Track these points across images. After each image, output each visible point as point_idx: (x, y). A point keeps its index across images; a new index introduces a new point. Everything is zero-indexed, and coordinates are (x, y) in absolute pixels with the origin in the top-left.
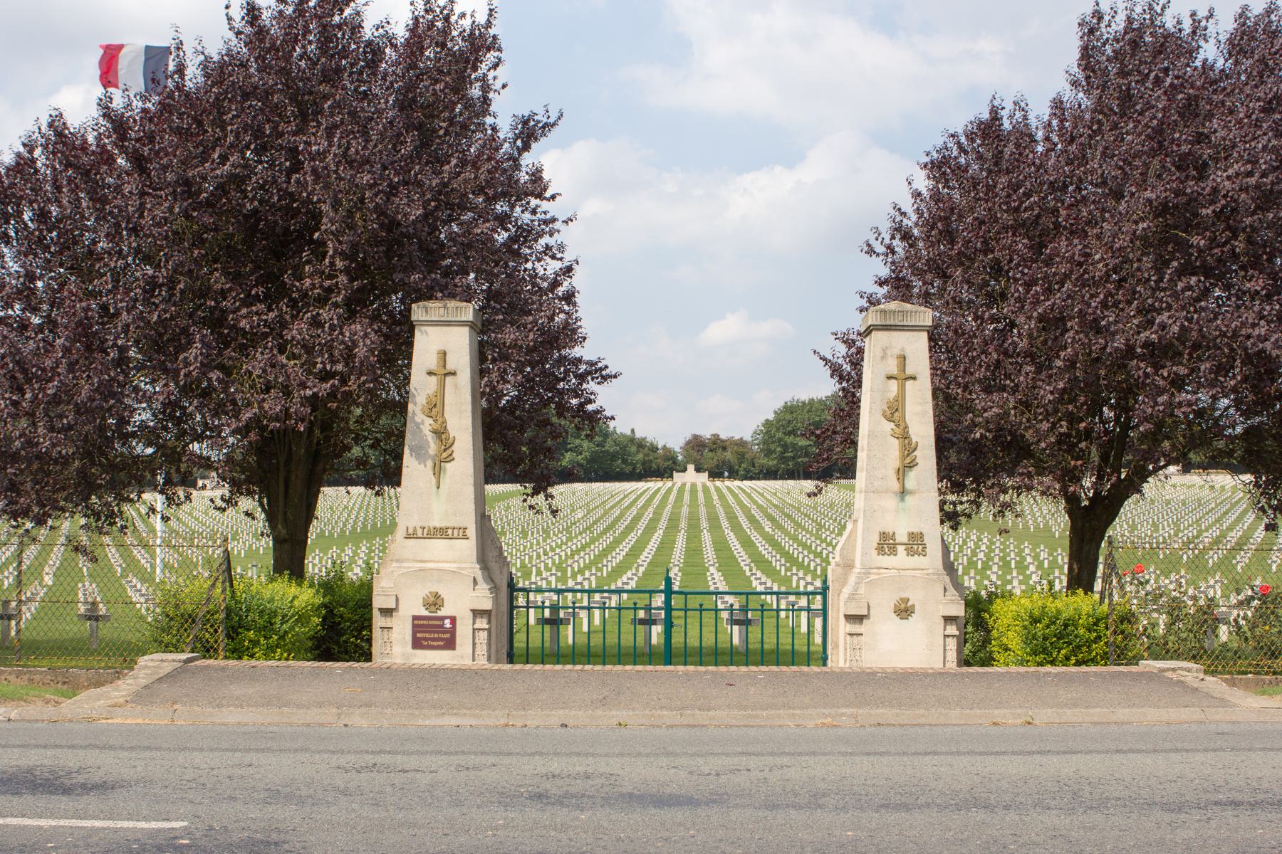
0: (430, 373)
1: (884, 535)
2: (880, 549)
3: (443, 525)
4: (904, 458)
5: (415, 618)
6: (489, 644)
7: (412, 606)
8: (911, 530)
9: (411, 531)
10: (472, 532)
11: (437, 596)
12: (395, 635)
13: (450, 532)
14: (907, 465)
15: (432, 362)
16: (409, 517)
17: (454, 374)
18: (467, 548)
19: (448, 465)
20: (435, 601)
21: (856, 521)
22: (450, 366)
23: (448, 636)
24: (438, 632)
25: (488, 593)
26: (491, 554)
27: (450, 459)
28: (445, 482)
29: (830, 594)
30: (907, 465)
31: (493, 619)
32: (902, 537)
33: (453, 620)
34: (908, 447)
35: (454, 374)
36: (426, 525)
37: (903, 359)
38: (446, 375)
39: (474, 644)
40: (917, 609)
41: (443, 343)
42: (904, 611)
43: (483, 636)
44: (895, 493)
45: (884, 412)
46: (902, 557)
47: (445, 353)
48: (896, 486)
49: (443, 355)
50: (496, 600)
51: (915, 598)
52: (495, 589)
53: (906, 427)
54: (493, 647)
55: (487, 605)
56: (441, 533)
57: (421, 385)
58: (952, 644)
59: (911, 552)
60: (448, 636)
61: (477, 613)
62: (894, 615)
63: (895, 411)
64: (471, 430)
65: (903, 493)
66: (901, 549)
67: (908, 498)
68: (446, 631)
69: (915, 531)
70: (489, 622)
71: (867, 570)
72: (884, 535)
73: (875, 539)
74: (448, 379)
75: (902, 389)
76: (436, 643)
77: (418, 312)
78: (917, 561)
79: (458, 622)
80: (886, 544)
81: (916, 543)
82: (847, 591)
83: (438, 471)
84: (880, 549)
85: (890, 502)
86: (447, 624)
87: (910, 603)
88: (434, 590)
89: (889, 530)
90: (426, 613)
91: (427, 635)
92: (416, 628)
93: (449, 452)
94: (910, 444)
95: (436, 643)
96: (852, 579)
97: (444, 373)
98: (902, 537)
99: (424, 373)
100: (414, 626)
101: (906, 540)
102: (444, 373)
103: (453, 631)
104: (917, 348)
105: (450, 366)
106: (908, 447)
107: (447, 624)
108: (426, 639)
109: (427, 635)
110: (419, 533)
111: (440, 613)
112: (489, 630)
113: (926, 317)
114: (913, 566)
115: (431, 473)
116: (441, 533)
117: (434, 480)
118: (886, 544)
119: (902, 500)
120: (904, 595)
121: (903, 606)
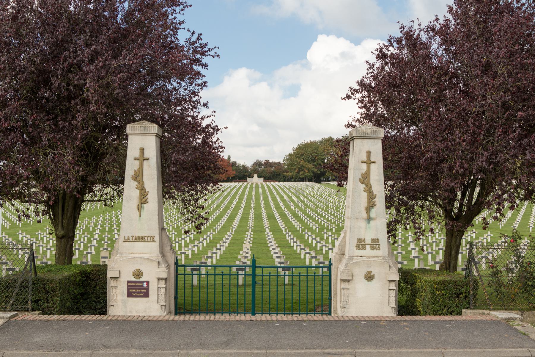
0: (136, 159)
1: (359, 240)
2: (358, 247)
3: (143, 235)
4: (369, 202)
5: (129, 282)
6: (166, 294)
7: (128, 276)
8: (373, 237)
9: (126, 238)
10: (157, 238)
11: (139, 270)
12: (119, 290)
13: (146, 238)
14: (371, 205)
15: (137, 154)
16: (127, 230)
17: (147, 159)
18: (155, 247)
19: (145, 205)
20: (138, 274)
21: (346, 232)
23: (145, 291)
24: (140, 289)
25: (165, 269)
26: (167, 248)
27: (146, 202)
29: (333, 267)
30: (371, 205)
31: (168, 281)
32: (368, 241)
33: (148, 283)
34: (371, 196)
35: (147, 159)
36: (134, 235)
37: (369, 153)
39: (158, 295)
40: (376, 276)
41: (142, 143)
42: (369, 277)
43: (163, 290)
44: (365, 219)
45: (360, 180)
46: (368, 251)
48: (365, 215)
49: (142, 150)
50: (169, 272)
51: (375, 271)
52: (168, 267)
53: (371, 187)
54: (168, 295)
55: (165, 275)
56: (141, 239)
58: (393, 294)
59: (373, 248)
60: (145, 291)
61: (159, 279)
62: (364, 280)
63: (365, 179)
64: (156, 188)
65: (369, 219)
66: (368, 247)
67: (371, 222)
68: (144, 288)
69: (375, 238)
70: (166, 283)
71: (351, 258)
72: (359, 240)
73: (356, 241)
74: (145, 162)
75: (369, 168)
76: (139, 295)
78: (375, 253)
79: (150, 284)
80: (361, 244)
81: (375, 244)
82: (342, 267)
83: (140, 208)
84: (358, 247)
85: (363, 224)
86: (145, 285)
87: (372, 274)
89: (363, 238)
90: (134, 279)
91: (135, 291)
92: (129, 287)
93: (145, 198)
94: (372, 195)
95: (139, 295)
96: (344, 261)
97: (142, 158)
98: (368, 241)
99: (133, 159)
100: (128, 286)
101: (370, 243)
102: (142, 158)
103: (147, 288)
104: (376, 148)
105: (146, 155)
106: (371, 196)
107: (145, 285)
108: (134, 293)
109: (135, 291)
110: (131, 239)
111: (141, 280)
112: (166, 288)
113: (381, 132)
114: (374, 255)
115: (137, 210)
116: (141, 239)
117: (138, 213)
118: (361, 244)
119: (369, 223)
120: (369, 270)
121: (369, 275)
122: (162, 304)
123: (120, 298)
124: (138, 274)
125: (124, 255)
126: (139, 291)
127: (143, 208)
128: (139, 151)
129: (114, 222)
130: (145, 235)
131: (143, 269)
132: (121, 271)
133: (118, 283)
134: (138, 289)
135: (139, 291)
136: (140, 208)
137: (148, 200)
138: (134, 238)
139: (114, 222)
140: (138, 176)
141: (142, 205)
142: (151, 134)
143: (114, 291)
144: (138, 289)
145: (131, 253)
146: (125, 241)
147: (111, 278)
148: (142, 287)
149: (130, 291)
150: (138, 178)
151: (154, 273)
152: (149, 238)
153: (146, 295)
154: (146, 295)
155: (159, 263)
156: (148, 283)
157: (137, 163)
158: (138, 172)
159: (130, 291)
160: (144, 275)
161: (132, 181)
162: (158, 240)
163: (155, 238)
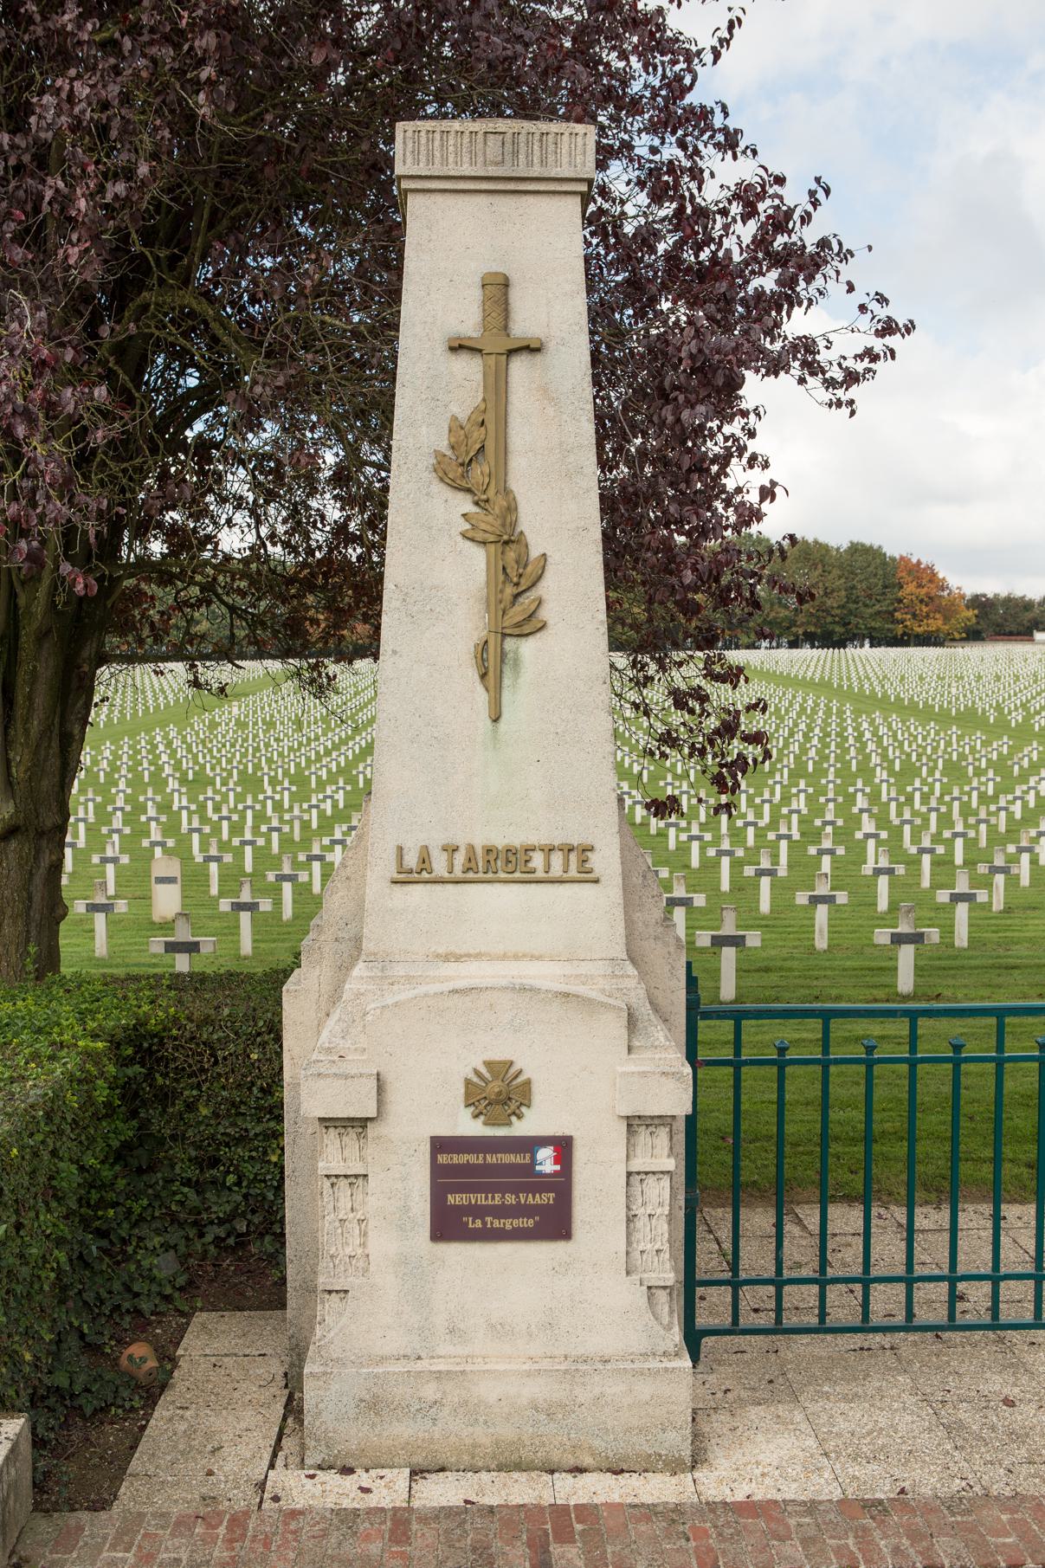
0: (458, 347)
3: (517, 839)
5: (440, 1145)
9: (411, 860)
10: (607, 860)
11: (500, 1069)
12: (375, 1199)
13: (538, 860)
15: (467, 319)
16: (407, 811)
19: (527, 649)
20: (500, 1092)
22: (524, 324)
23: (548, 1198)
24: (516, 1189)
27: (530, 625)
28: (519, 698)
33: (563, 1147)
36: (462, 842)
38: (511, 352)
39: (631, 1219)
47: (506, 284)
49: (498, 290)
56: (504, 864)
57: (430, 391)
60: (548, 1198)
61: (634, 1123)
68: (542, 1184)
74: (519, 366)
76: (508, 1224)
77: (417, 147)
79: (580, 1156)
83: (492, 666)
86: (546, 1161)
88: (498, 1055)
90: (469, 1126)
91: (480, 1199)
93: (526, 600)
95: (508, 1224)
97: (500, 345)
99: (441, 348)
100: (437, 1171)
102: (500, 345)
103: (562, 1185)
105: (524, 324)
107: (546, 1161)
108: (478, 1211)
109: (480, 1199)
110: (439, 866)
115: (473, 674)
116: (504, 864)
117: (481, 697)
122: (654, 1278)
123: (382, 1245)
124: (500, 1092)
125: (399, 970)
126: (510, 1199)
127: (517, 663)
128: (476, 293)
129: (850, 730)
130: (533, 840)
131: (529, 1064)
132: (389, 1078)
133: (371, 1150)
134: (503, 1189)
135: (510, 1199)
136: (492, 666)
137: (545, 614)
138: (460, 858)
139: (850, 730)
140: (475, 461)
141: (510, 644)
142: (551, 186)
143: (345, 1202)
144: (498, 1188)
145: (447, 958)
146: (406, 877)
147: (327, 1122)
148: (527, 1177)
149: (451, 1199)
150: (478, 472)
151: (612, 1093)
152: (557, 859)
153: (555, 1224)
154: (555, 1224)
155: (632, 1022)
156: (563, 1147)
157: (469, 369)
158: (478, 434)
159: (451, 1199)
160: (537, 1097)
161: (439, 489)
162: (616, 868)
163: (595, 860)
